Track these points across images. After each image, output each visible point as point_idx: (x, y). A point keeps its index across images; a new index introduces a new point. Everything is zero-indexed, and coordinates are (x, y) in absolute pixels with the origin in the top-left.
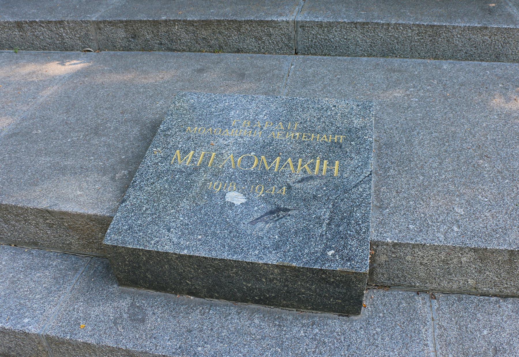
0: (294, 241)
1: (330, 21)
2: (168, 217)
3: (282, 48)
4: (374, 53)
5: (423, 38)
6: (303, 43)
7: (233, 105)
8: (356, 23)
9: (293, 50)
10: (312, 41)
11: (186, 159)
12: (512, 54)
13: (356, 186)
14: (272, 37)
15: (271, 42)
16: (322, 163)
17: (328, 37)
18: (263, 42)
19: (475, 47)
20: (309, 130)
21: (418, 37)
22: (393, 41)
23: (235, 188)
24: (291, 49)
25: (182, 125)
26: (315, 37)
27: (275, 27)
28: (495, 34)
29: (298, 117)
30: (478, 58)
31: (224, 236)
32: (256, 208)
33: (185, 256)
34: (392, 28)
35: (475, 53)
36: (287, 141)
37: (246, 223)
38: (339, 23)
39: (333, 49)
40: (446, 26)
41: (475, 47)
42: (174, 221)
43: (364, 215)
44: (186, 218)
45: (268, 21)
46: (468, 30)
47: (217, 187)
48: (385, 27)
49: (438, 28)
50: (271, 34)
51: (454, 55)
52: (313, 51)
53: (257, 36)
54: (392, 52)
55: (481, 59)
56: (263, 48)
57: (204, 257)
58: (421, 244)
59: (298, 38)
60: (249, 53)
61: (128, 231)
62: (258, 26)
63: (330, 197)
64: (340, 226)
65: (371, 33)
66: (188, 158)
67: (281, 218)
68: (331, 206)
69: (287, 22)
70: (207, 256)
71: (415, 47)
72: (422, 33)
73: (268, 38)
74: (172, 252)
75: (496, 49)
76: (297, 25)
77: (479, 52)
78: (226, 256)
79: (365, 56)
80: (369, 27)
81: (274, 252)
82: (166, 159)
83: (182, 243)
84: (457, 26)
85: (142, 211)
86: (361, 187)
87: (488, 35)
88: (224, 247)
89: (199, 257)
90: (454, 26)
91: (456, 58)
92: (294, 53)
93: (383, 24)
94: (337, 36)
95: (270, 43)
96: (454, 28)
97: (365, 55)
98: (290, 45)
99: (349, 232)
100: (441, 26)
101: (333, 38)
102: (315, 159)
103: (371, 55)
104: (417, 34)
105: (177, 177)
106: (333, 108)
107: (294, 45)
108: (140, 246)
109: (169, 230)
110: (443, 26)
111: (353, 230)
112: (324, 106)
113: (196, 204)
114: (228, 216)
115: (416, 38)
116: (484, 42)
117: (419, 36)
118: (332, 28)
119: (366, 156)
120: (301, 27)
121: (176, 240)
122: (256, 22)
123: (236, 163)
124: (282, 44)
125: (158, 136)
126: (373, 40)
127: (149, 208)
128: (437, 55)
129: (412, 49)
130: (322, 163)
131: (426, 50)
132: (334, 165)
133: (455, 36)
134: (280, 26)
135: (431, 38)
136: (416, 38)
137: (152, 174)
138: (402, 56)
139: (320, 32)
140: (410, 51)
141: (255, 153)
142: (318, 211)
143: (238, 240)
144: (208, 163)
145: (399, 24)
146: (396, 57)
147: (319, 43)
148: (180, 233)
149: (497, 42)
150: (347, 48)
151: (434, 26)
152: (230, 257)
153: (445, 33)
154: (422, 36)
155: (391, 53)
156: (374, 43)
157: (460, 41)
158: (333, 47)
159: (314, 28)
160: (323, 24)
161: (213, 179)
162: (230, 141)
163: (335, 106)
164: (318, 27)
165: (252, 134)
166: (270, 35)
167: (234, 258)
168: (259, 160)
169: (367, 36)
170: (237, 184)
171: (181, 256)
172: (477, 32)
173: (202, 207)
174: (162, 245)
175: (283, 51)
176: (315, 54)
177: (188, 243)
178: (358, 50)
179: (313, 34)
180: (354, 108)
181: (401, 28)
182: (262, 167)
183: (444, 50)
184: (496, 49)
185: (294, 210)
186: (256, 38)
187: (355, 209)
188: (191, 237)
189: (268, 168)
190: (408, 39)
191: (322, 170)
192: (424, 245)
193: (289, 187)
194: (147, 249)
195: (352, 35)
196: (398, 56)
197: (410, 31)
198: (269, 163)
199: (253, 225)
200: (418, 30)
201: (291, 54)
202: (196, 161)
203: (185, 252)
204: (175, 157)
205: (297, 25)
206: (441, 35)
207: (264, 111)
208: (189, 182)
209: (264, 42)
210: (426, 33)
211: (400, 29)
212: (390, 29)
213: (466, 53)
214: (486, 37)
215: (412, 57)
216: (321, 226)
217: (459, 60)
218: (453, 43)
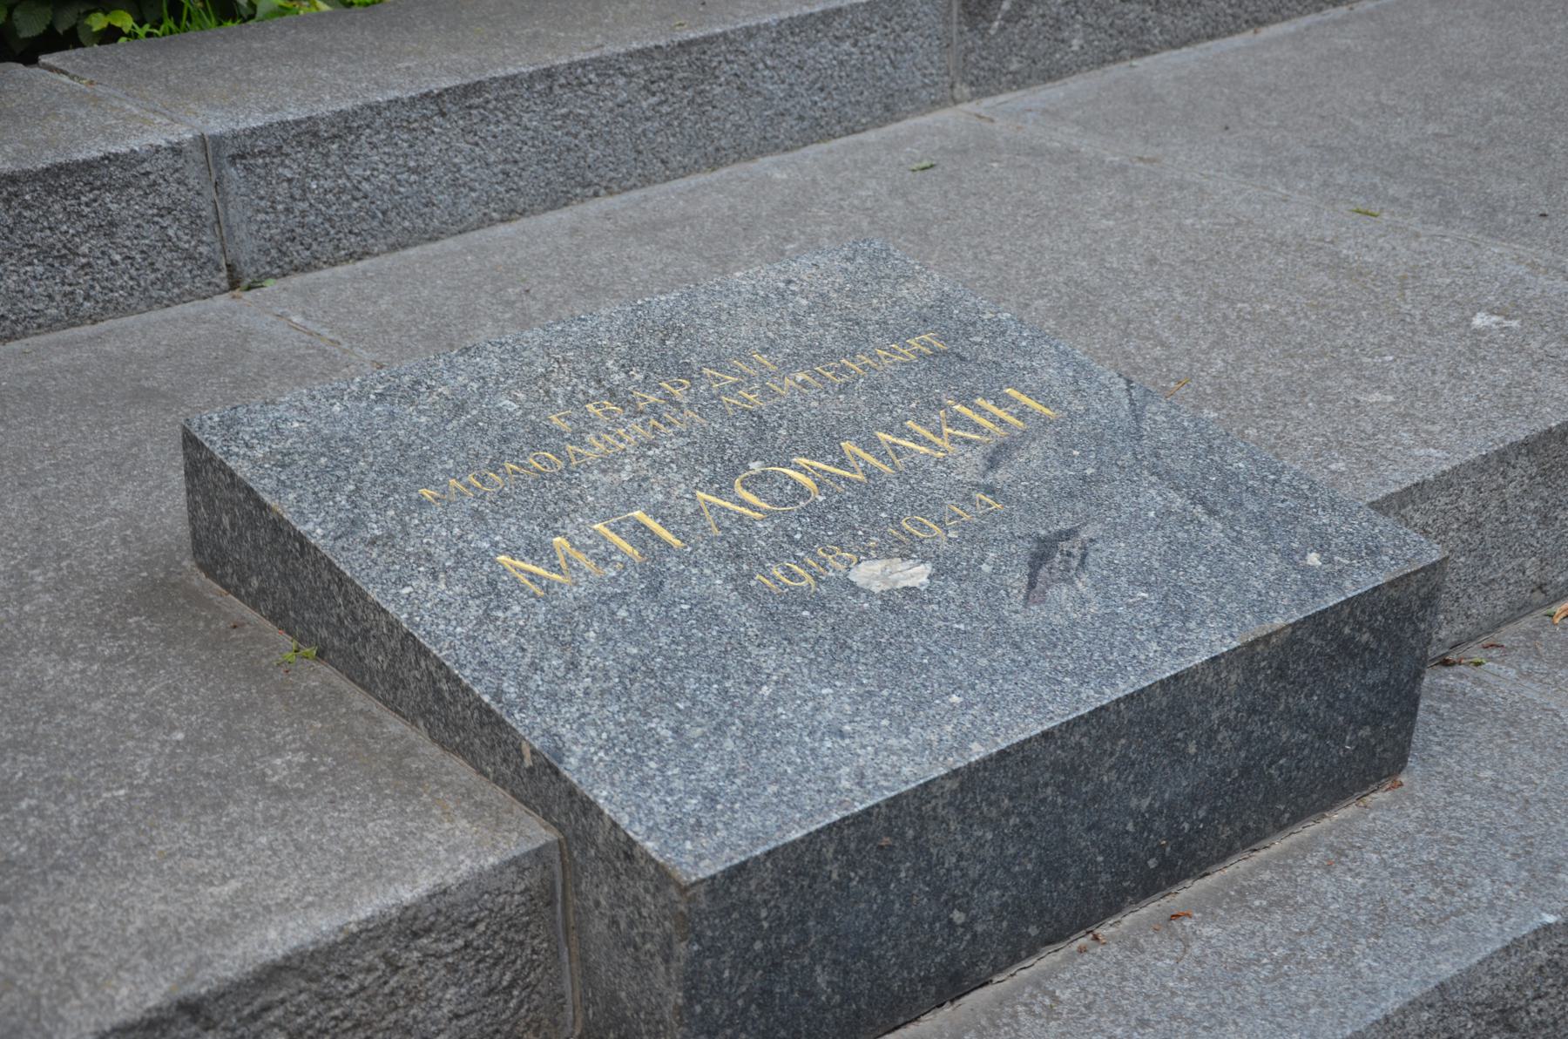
0: (1194, 580)
1: (343, 107)
2: (780, 710)
3: (170, 274)
4: (522, 202)
5: (666, 101)
6: (254, 227)
7: (475, 386)
8: (440, 95)
9: (219, 270)
10: (288, 210)
11: (570, 565)
12: (925, 86)
13: (1138, 418)
14: (121, 236)
15: (118, 258)
16: (981, 411)
17: (348, 178)
18: (82, 267)
19: (822, 89)
20: (814, 355)
21: (653, 100)
22: (576, 136)
23: (846, 555)
24: (210, 266)
25: (387, 496)
26: (297, 193)
27: (128, 185)
28: (866, 28)
29: (735, 341)
30: (838, 128)
31: (1013, 661)
32: (986, 568)
33: (984, 764)
34: (561, 86)
35: (824, 110)
36: (798, 400)
37: (1020, 608)
38: (376, 109)
39: (375, 223)
40: (724, 35)
41: (822, 89)
42: (816, 709)
43: (1255, 460)
44: (838, 683)
45: (88, 165)
46: (792, 33)
47: (791, 575)
48: (538, 87)
49: (705, 46)
50: (112, 224)
51: (769, 135)
52: (299, 254)
53: (52, 247)
54: (578, 179)
55: (846, 129)
56: (87, 297)
57: (1046, 735)
58: (1416, 485)
59: (231, 211)
60: (25, 335)
61: (719, 807)
62: (49, 194)
63: (1119, 463)
64: (1241, 505)
65: (498, 123)
66: (567, 557)
67: (1084, 556)
68: (1154, 479)
69: (176, 150)
70: (1048, 726)
71: (650, 142)
72: (661, 79)
73: (104, 241)
74: (943, 771)
75: (880, 79)
76: (217, 155)
77: (836, 104)
78: (1092, 698)
79: (492, 222)
80: (488, 102)
81: (1192, 625)
82: (498, 595)
83: (934, 738)
84: (758, 27)
85: (671, 740)
86: (1155, 414)
87: (848, 37)
88: (1060, 683)
89: (1030, 740)
90: (747, 28)
91: (777, 147)
92: (225, 284)
93: (531, 76)
94: (381, 166)
95: (114, 263)
96: (750, 34)
97: (491, 219)
98: (203, 249)
99: (1280, 505)
100: (709, 40)
101: (367, 179)
102: (941, 406)
103: (512, 211)
104: (645, 87)
105: (622, 613)
106: (793, 287)
107: (218, 246)
108: (827, 815)
109: (842, 735)
110: (717, 36)
111: (1282, 497)
112: (762, 293)
113: (806, 640)
114: (946, 619)
115: (644, 104)
116: (841, 63)
117: (654, 94)
118: (358, 138)
119: (1053, 351)
120: (233, 159)
121: (905, 741)
122: (33, 177)
123: (743, 503)
124: (169, 256)
125: (344, 554)
126: (507, 149)
127: (682, 723)
128: (717, 150)
129: (639, 152)
130: (981, 411)
131: (686, 142)
132: (1016, 401)
133: (761, 66)
134: (147, 174)
135: (690, 93)
136: (644, 104)
137: (523, 650)
138: (616, 189)
139: (316, 164)
140: (635, 159)
141: (758, 463)
142: (1141, 500)
143: (1064, 650)
144: (659, 540)
145: (583, 64)
146: (596, 195)
147: (319, 213)
148: (885, 722)
149: (878, 53)
150: (426, 205)
151: (691, 43)
152: (1110, 695)
153: (728, 62)
154: (663, 91)
155: (579, 184)
156: (516, 162)
157: (776, 78)
158: (374, 217)
159: (287, 155)
160: (322, 127)
161: (745, 567)
162: (628, 468)
163: (789, 282)
164: (300, 143)
165: (670, 424)
166: (110, 227)
167: (1123, 688)
168: (801, 470)
169: (484, 139)
170: (839, 544)
171: (972, 769)
172: (818, 31)
173: (837, 639)
174: (885, 775)
175: (178, 285)
176: (308, 264)
177: (949, 728)
178: (464, 204)
179: (290, 181)
180: (851, 268)
181: (592, 76)
182: (839, 483)
183: (738, 127)
184: (880, 79)
185: (1085, 524)
186: (44, 253)
187: (1217, 458)
188: (932, 712)
189: (860, 477)
190: (622, 115)
191: (1002, 421)
192: (1424, 483)
193: (990, 490)
194: (859, 807)
195: (435, 149)
196: (602, 192)
197: (621, 81)
198: (843, 464)
199: (1043, 601)
200: (647, 70)
201: (213, 291)
202: (611, 554)
203: (977, 752)
204: (522, 578)
205: (217, 155)
206: (717, 73)
207: (603, 362)
208: (686, 607)
209: (89, 265)
210: (671, 76)
211: (590, 82)
212: (557, 90)
213: (801, 118)
214: (846, 46)
215: (647, 181)
216: (1201, 525)
217: (786, 150)
218: (758, 93)
